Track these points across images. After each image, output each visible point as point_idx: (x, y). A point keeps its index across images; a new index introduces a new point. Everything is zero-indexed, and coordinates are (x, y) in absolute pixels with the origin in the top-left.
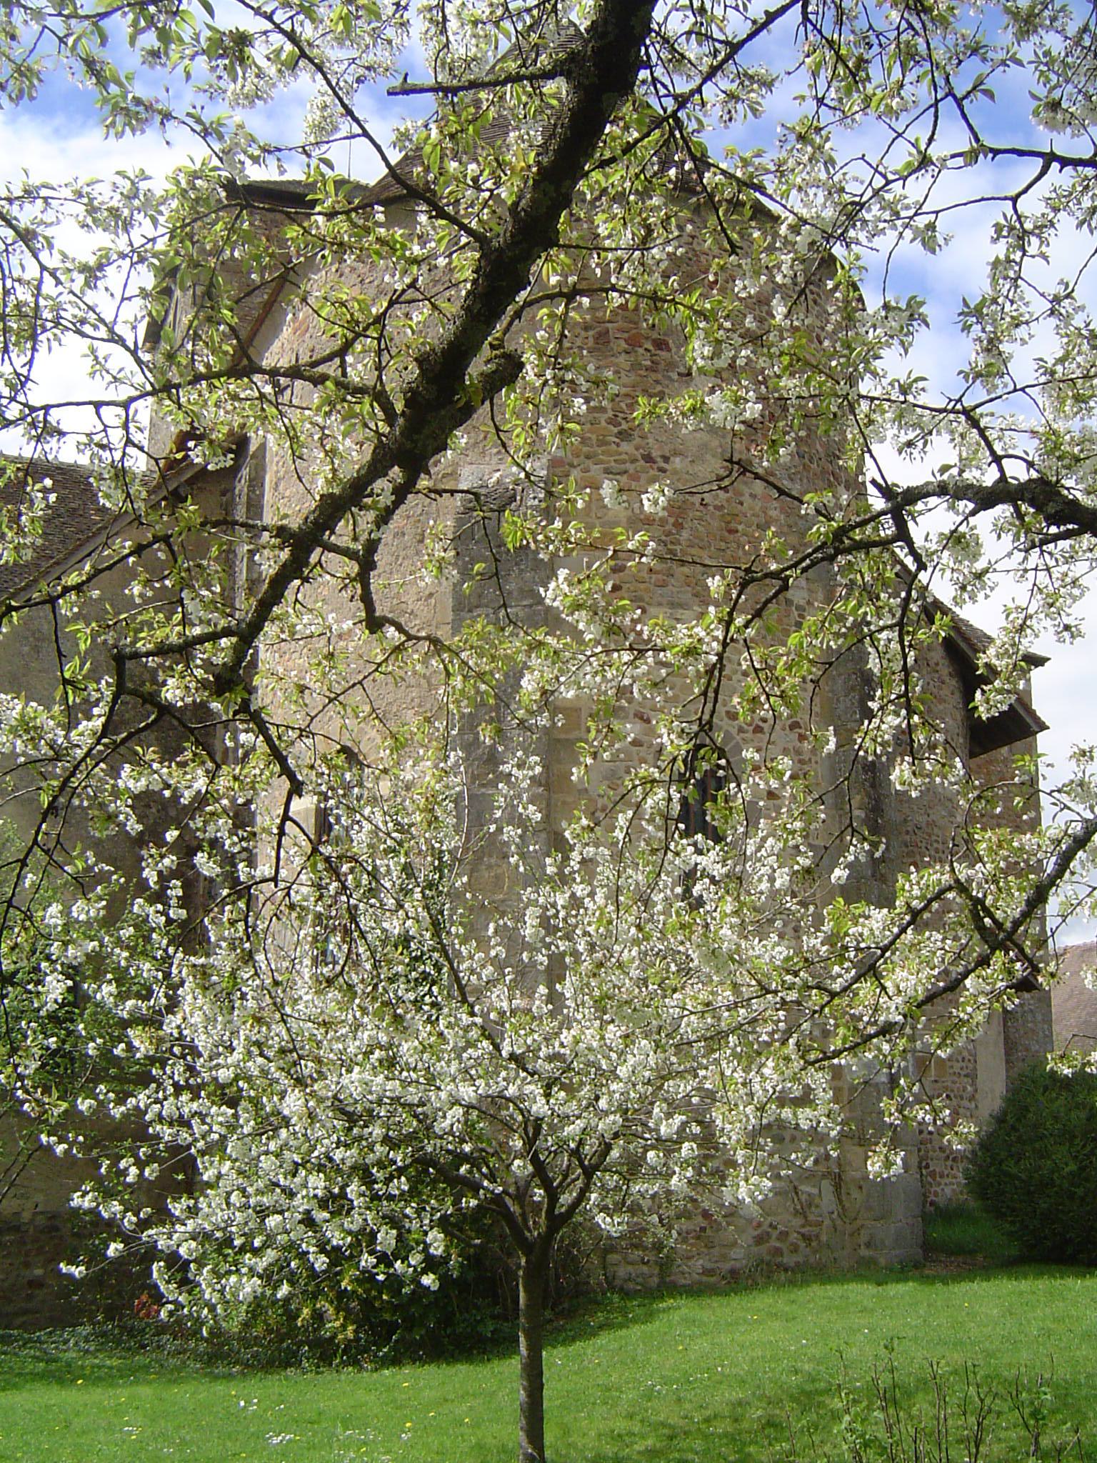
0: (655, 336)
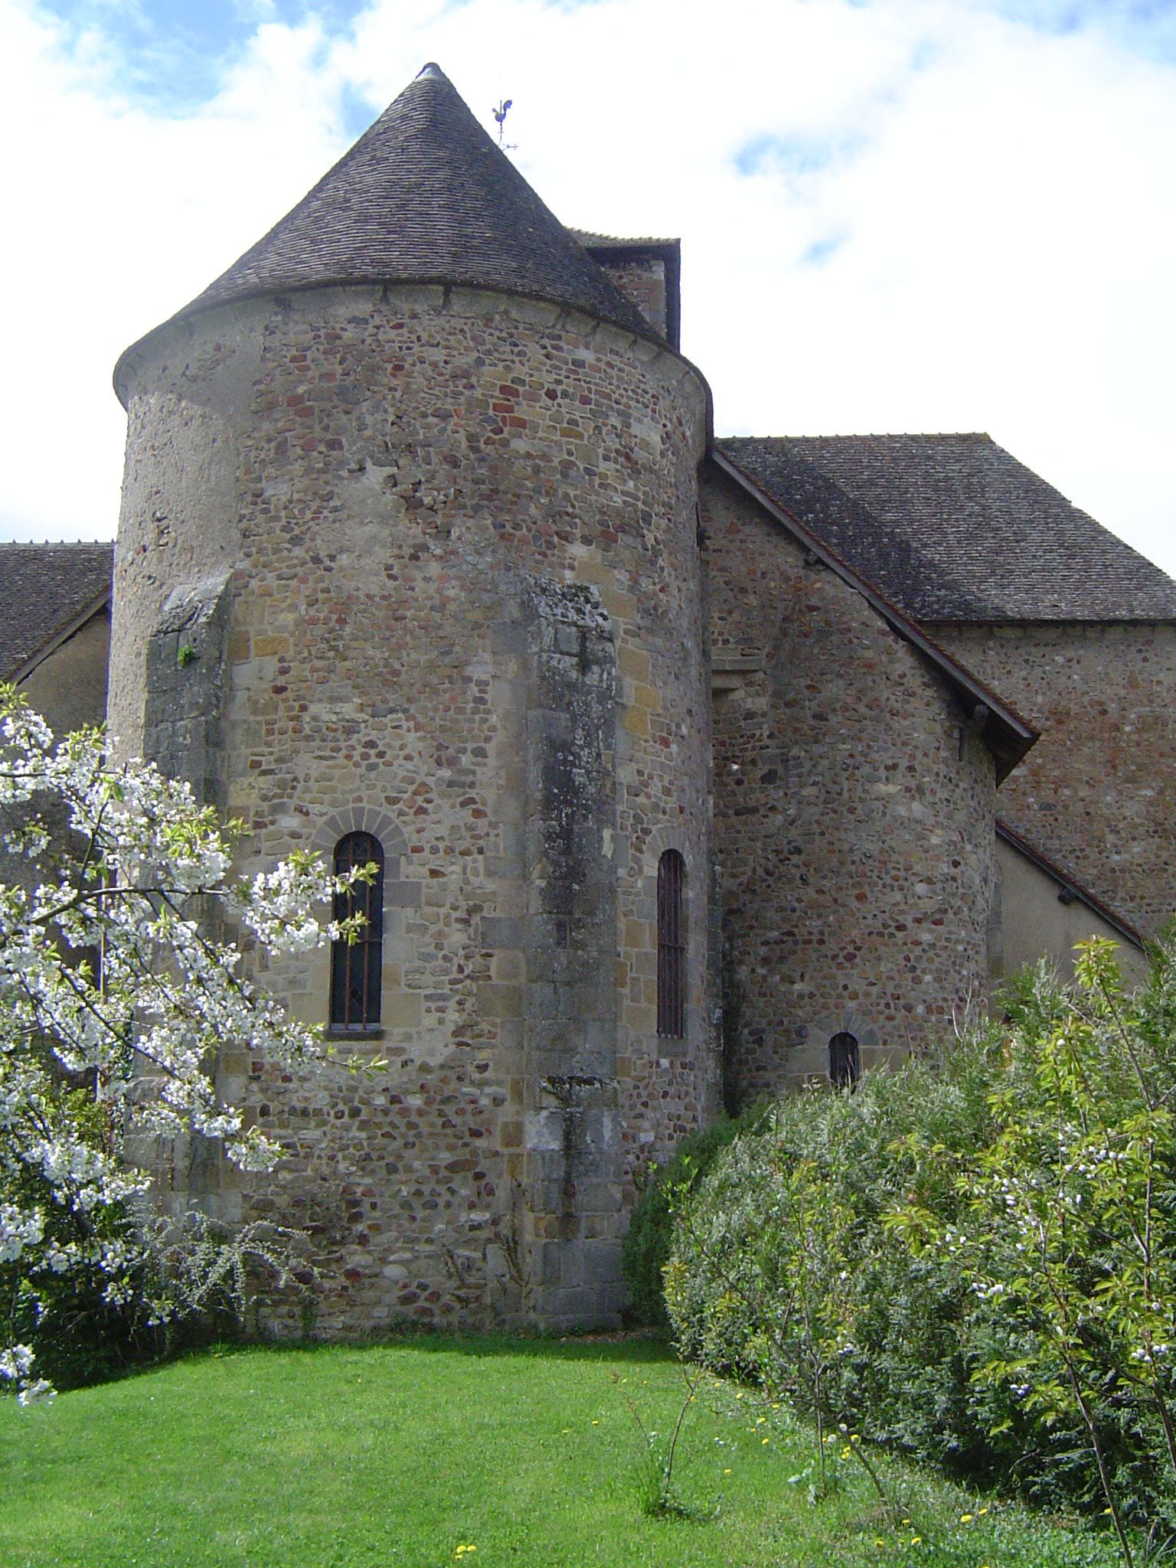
0: (329, 436)
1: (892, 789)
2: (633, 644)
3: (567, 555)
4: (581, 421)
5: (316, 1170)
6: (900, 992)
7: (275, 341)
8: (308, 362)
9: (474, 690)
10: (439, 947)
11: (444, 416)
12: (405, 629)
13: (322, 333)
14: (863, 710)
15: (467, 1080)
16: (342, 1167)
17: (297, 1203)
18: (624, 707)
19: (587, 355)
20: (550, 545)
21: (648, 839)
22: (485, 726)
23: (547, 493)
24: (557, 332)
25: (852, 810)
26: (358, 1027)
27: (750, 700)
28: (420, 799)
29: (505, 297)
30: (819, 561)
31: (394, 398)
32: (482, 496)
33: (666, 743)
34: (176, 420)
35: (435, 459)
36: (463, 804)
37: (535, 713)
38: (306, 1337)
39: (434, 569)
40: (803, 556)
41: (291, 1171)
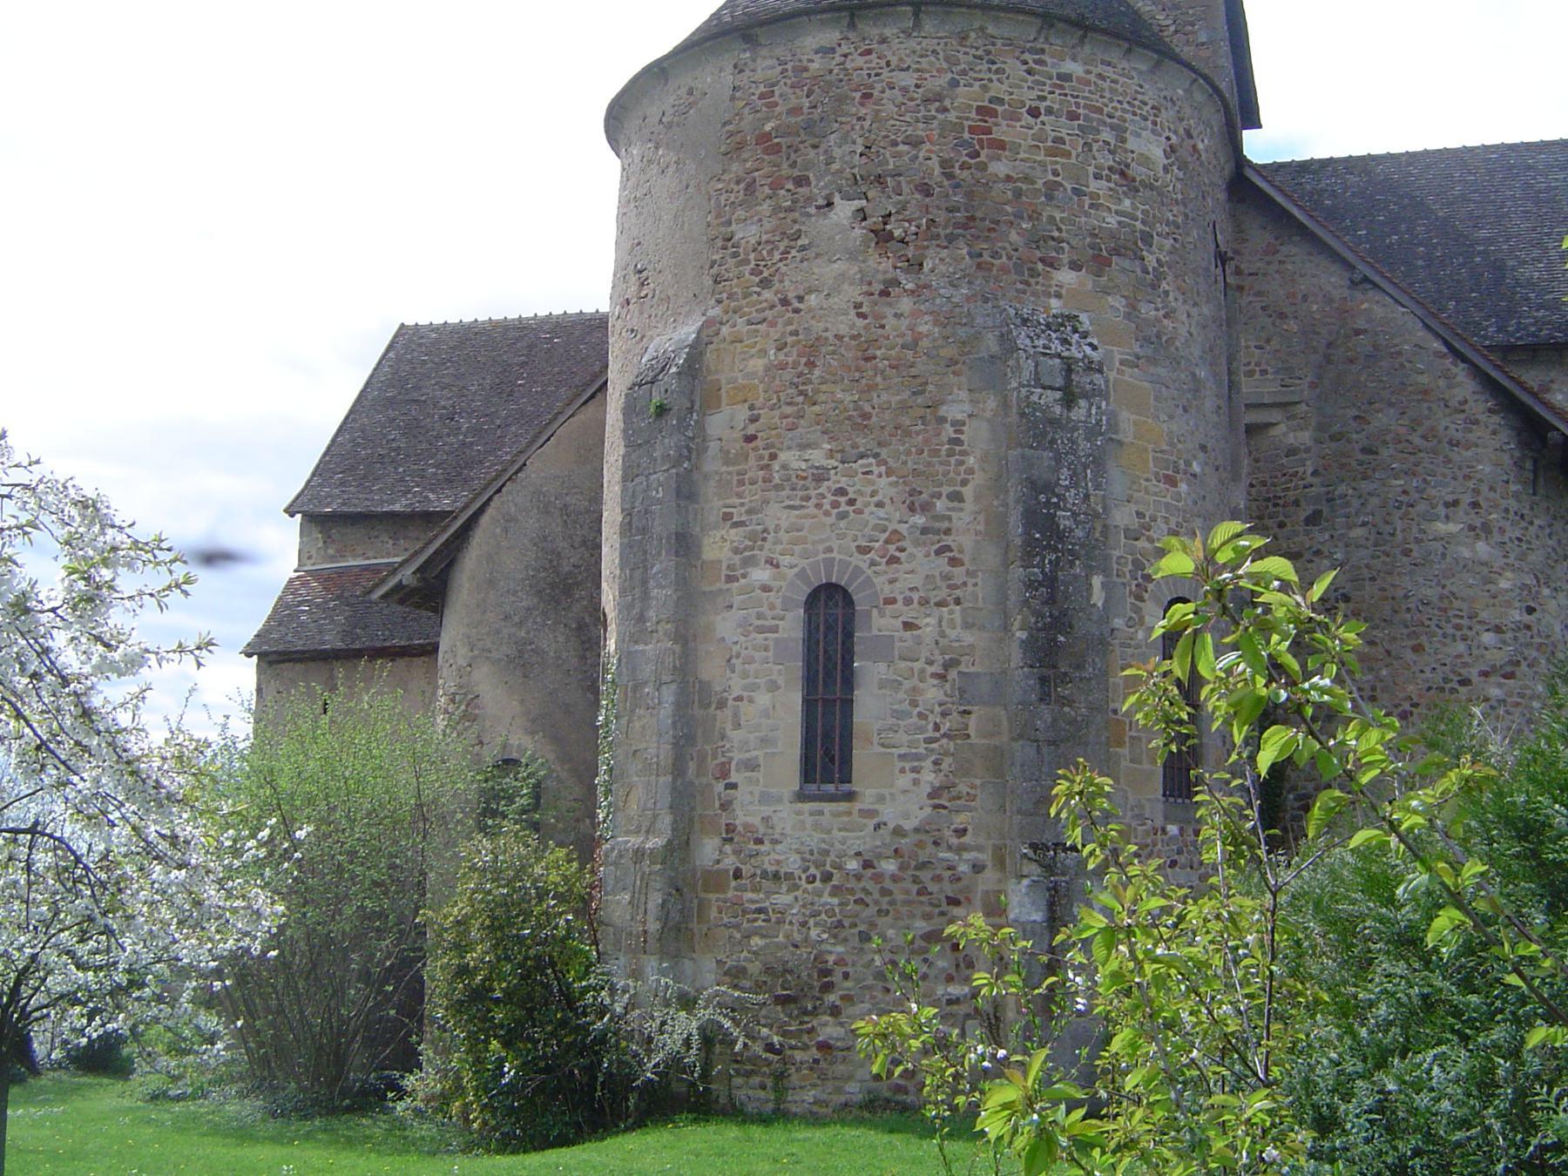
0: (796, 173)
1: (1453, 528)
2: (1130, 375)
3: (1053, 283)
4: (1067, 138)
5: (787, 937)
7: (743, 80)
8: (776, 98)
9: (949, 431)
10: (914, 704)
11: (915, 143)
12: (875, 368)
13: (789, 67)
14: (1417, 441)
15: (944, 845)
16: (814, 933)
17: (768, 970)
18: (1120, 443)
19: (1074, 68)
20: (1034, 273)
21: (1150, 587)
22: (962, 468)
23: (1030, 218)
24: (1039, 46)
25: (1407, 553)
26: (830, 788)
27: (1291, 435)
28: (892, 548)
29: (979, 13)
30: (1366, 279)
31: (862, 127)
32: (957, 225)
33: (1172, 482)
34: (655, 169)
35: (906, 189)
36: (938, 552)
37: (1015, 453)
38: (776, 1110)
39: (906, 304)
40: (1347, 275)
41: (763, 936)
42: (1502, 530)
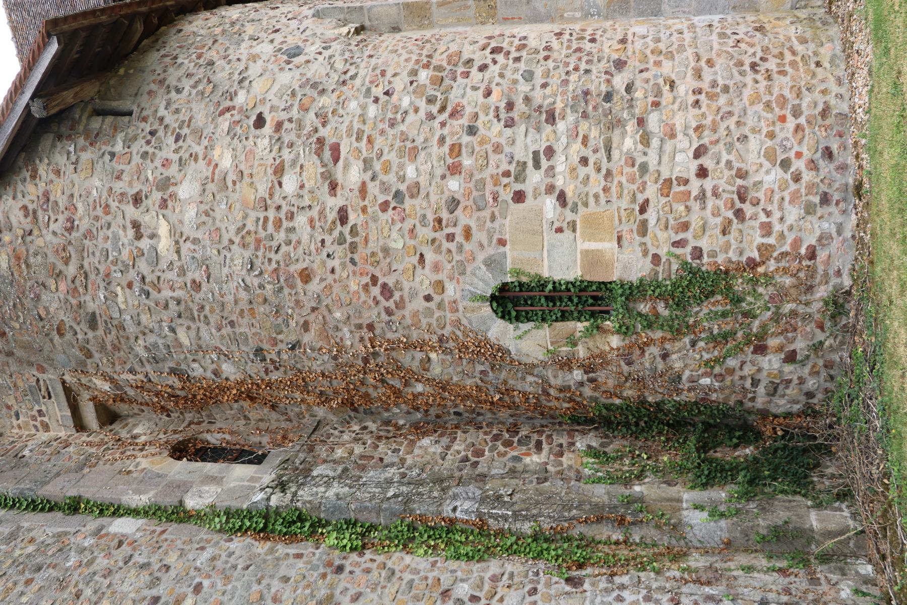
1: (163, 229)
6: (430, 217)
14: (72, 270)
25: (197, 286)
42: (166, 163)
